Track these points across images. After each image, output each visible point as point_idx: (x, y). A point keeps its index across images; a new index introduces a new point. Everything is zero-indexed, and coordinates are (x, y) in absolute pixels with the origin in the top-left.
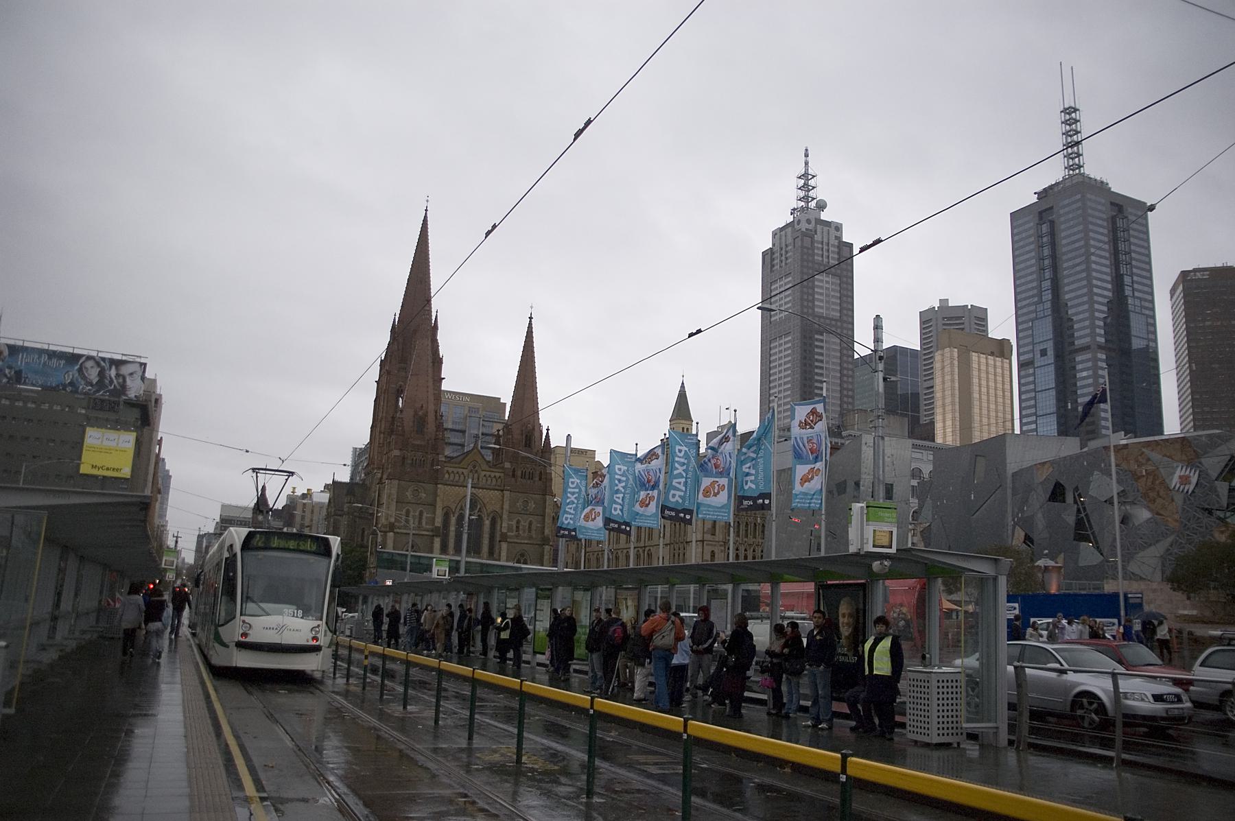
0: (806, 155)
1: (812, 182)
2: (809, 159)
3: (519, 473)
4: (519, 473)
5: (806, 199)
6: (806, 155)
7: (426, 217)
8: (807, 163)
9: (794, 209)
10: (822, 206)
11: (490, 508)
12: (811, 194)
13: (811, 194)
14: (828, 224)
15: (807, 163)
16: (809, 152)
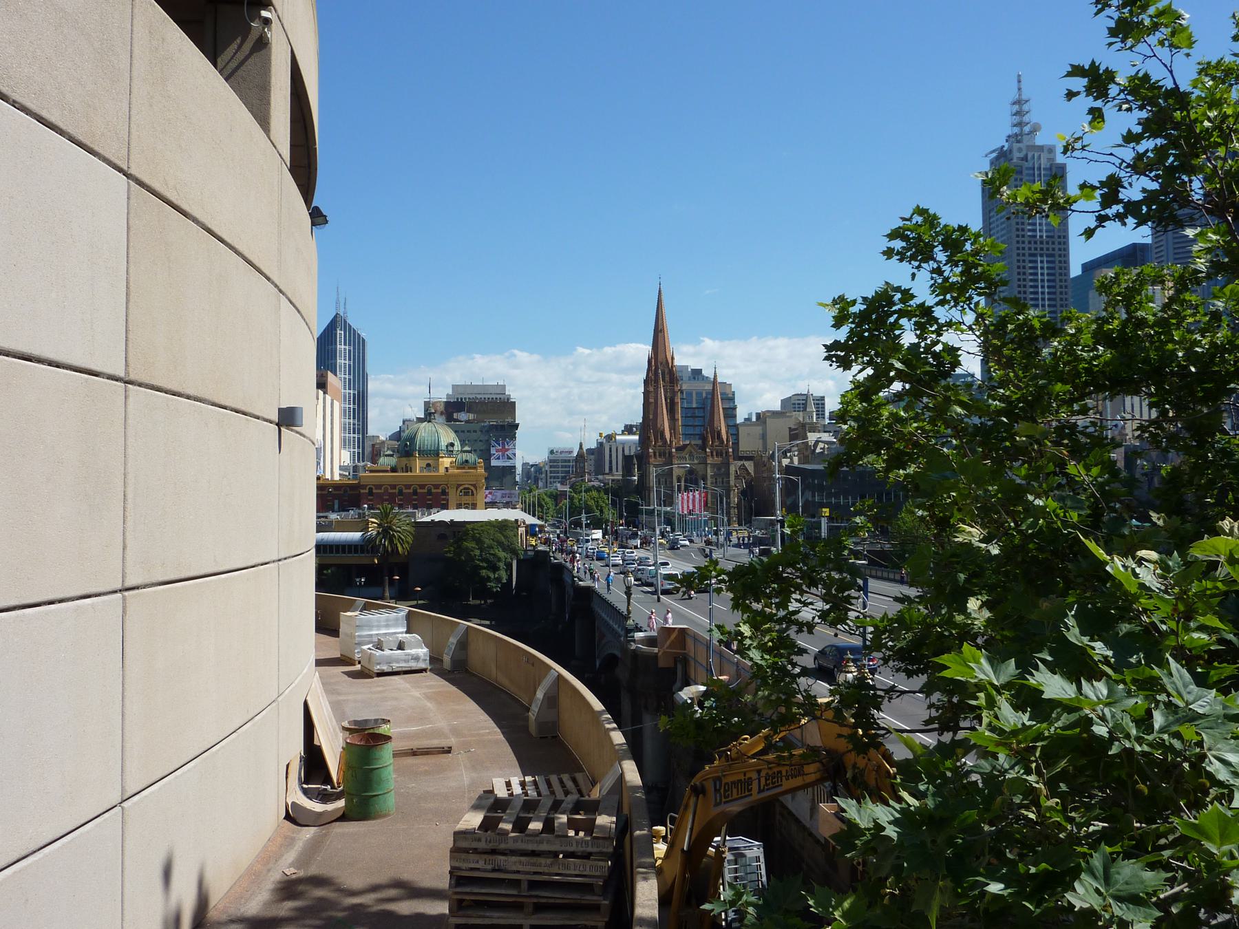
0: (1019, 81)
1: (1025, 107)
2: (1023, 85)
3: (715, 454)
4: (715, 454)
5: (1020, 124)
6: (1019, 81)
7: (660, 291)
8: (1019, 89)
9: (1009, 136)
10: (1035, 129)
11: (701, 473)
12: (1026, 119)
13: (1026, 119)
14: (1041, 148)
15: (1019, 89)
16: (1022, 79)
